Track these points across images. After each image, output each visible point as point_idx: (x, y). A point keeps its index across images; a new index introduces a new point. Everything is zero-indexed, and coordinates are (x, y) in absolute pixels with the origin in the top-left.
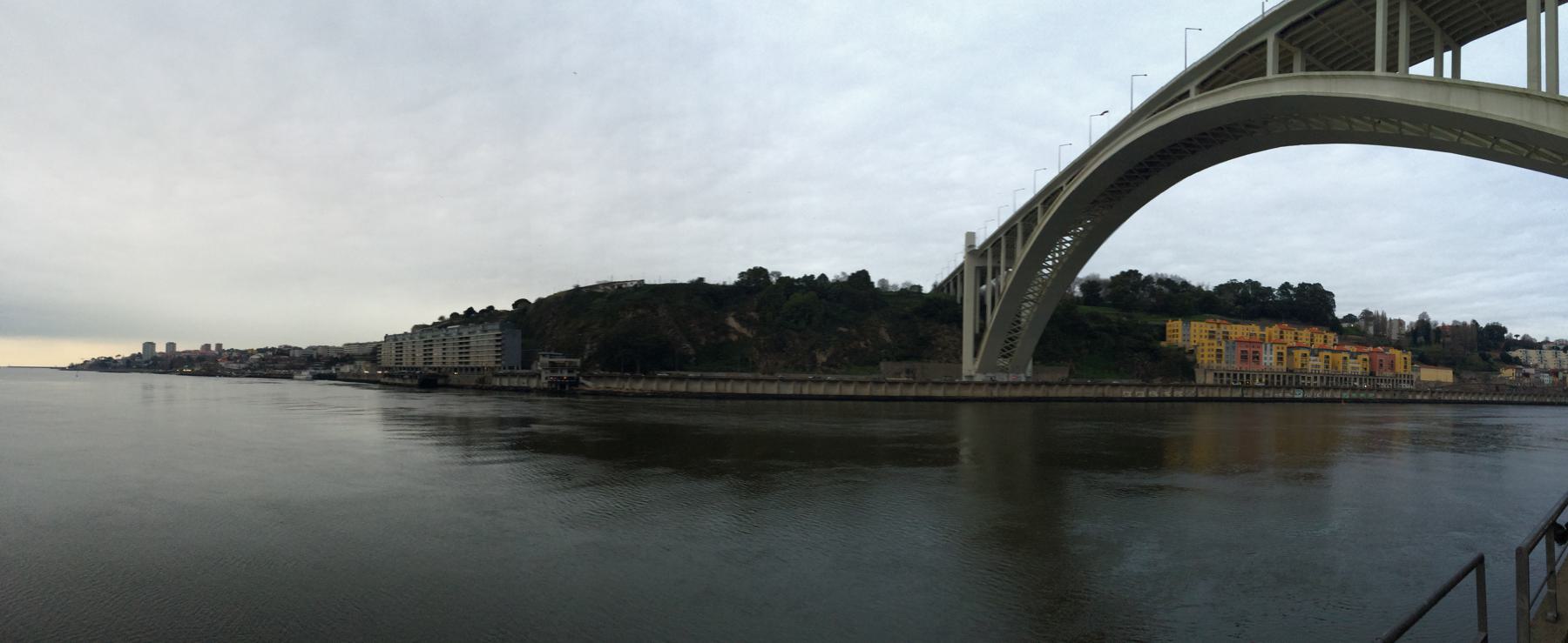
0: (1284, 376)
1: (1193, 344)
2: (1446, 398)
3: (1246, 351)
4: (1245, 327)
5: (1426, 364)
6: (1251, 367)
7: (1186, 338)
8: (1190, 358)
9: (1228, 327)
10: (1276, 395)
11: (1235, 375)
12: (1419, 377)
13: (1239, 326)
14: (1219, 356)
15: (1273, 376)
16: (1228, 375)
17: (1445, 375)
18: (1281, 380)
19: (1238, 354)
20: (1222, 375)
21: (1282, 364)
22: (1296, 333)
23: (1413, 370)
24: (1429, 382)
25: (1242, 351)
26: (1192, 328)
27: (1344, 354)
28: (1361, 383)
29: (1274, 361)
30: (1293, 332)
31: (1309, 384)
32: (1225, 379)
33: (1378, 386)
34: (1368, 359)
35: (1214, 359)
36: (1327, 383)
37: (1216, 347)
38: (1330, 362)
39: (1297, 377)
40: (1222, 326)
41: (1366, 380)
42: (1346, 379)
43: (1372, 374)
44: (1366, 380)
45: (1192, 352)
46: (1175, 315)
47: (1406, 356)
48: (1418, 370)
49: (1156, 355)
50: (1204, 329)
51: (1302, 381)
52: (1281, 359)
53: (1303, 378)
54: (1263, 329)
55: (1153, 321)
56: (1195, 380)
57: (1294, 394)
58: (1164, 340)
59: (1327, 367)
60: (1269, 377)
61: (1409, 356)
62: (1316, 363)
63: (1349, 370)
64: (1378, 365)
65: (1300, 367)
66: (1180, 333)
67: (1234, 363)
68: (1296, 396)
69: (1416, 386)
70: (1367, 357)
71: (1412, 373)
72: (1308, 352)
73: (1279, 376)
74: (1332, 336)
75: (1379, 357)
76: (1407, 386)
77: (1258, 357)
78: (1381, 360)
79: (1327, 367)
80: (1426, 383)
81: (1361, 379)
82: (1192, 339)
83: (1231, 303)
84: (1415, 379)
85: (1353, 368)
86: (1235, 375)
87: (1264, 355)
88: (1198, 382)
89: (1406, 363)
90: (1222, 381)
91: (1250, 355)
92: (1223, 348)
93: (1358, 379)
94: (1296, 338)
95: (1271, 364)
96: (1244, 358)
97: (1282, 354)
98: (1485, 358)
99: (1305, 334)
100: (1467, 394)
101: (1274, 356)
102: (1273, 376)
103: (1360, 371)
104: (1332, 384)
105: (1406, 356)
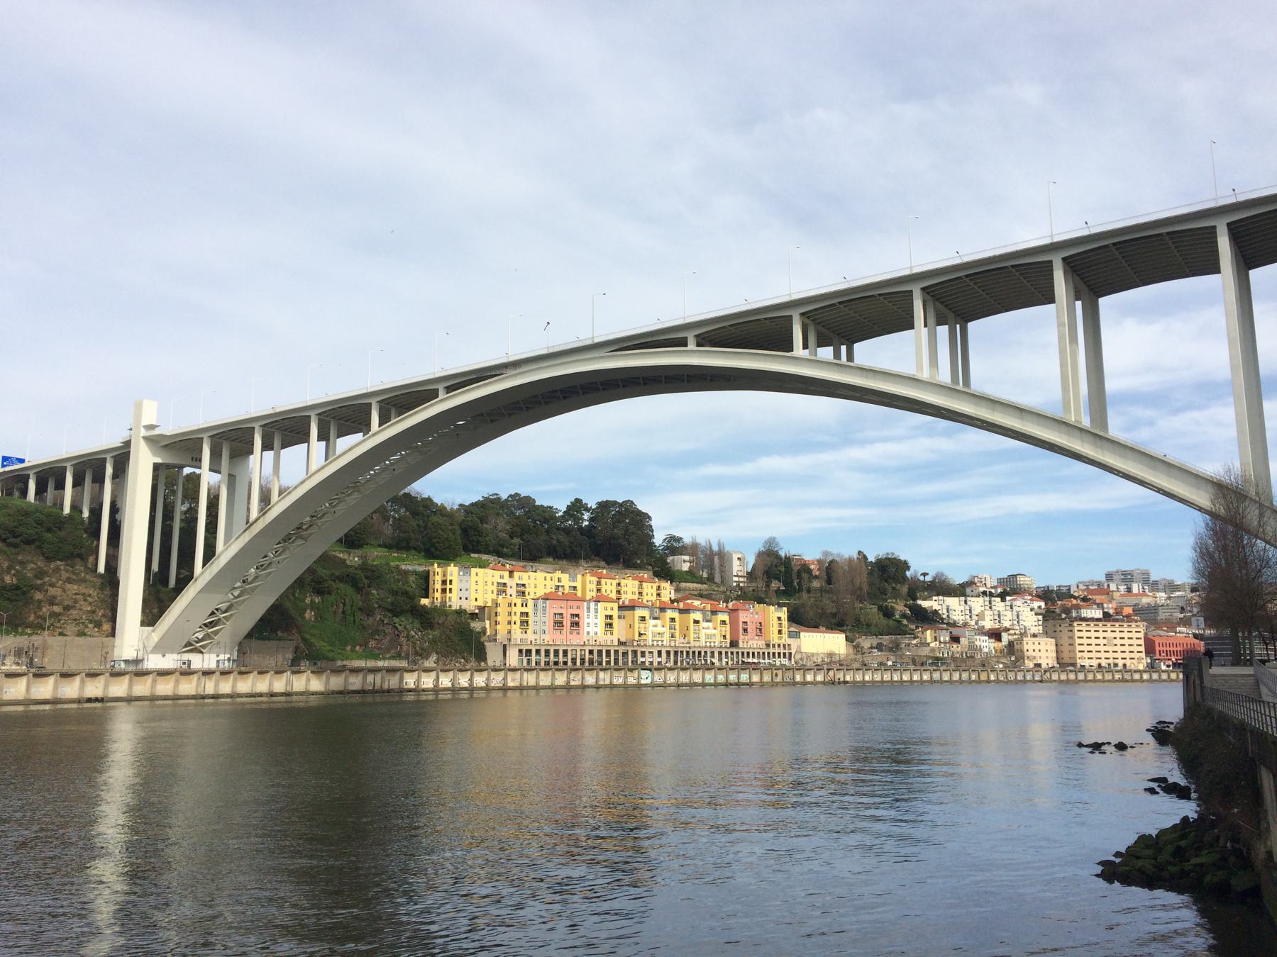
0: (616, 652)
1: (474, 603)
3: (562, 614)
4: (549, 576)
5: (808, 626)
6: (564, 639)
7: (464, 594)
8: (476, 625)
9: (525, 575)
10: (615, 682)
11: (547, 652)
12: (799, 647)
13: (540, 575)
14: (525, 623)
15: (600, 652)
16: (538, 652)
18: (612, 658)
19: (549, 620)
20: (529, 652)
21: (612, 634)
22: (619, 584)
23: (790, 636)
24: (813, 655)
26: (473, 577)
27: (698, 616)
28: (720, 659)
29: (601, 628)
30: (615, 582)
31: (651, 663)
32: (534, 657)
33: (743, 661)
34: (728, 622)
35: (516, 629)
36: (676, 662)
37: (519, 609)
38: (677, 627)
39: (635, 652)
40: (516, 574)
41: (726, 653)
42: (700, 653)
43: (734, 644)
44: (726, 653)
45: (474, 616)
46: (446, 555)
47: (779, 614)
49: (426, 618)
50: (490, 580)
51: (641, 659)
52: (611, 625)
53: (643, 654)
54: (573, 579)
55: (413, 565)
56: (485, 660)
57: (639, 678)
58: (427, 596)
59: (673, 636)
60: (595, 653)
61: (783, 613)
62: (656, 632)
63: (703, 639)
64: (741, 631)
65: (637, 637)
66: (455, 587)
67: (544, 632)
68: (643, 682)
70: (725, 617)
72: (646, 613)
73: (608, 652)
74: (668, 591)
76: (785, 661)
77: (577, 624)
78: (745, 623)
79: (673, 636)
80: (809, 656)
81: (720, 653)
82: (473, 596)
83: (504, 535)
84: (793, 651)
85: (708, 636)
86: (547, 652)
87: (586, 621)
88: (490, 663)
90: (529, 662)
91: (567, 622)
92: (530, 609)
93: (716, 655)
94: (618, 592)
95: (596, 633)
96: (558, 624)
97: (611, 617)
98: (888, 613)
99: (630, 585)
101: (601, 621)
102: (600, 652)
103: (717, 641)
104: (682, 662)
105: (779, 614)
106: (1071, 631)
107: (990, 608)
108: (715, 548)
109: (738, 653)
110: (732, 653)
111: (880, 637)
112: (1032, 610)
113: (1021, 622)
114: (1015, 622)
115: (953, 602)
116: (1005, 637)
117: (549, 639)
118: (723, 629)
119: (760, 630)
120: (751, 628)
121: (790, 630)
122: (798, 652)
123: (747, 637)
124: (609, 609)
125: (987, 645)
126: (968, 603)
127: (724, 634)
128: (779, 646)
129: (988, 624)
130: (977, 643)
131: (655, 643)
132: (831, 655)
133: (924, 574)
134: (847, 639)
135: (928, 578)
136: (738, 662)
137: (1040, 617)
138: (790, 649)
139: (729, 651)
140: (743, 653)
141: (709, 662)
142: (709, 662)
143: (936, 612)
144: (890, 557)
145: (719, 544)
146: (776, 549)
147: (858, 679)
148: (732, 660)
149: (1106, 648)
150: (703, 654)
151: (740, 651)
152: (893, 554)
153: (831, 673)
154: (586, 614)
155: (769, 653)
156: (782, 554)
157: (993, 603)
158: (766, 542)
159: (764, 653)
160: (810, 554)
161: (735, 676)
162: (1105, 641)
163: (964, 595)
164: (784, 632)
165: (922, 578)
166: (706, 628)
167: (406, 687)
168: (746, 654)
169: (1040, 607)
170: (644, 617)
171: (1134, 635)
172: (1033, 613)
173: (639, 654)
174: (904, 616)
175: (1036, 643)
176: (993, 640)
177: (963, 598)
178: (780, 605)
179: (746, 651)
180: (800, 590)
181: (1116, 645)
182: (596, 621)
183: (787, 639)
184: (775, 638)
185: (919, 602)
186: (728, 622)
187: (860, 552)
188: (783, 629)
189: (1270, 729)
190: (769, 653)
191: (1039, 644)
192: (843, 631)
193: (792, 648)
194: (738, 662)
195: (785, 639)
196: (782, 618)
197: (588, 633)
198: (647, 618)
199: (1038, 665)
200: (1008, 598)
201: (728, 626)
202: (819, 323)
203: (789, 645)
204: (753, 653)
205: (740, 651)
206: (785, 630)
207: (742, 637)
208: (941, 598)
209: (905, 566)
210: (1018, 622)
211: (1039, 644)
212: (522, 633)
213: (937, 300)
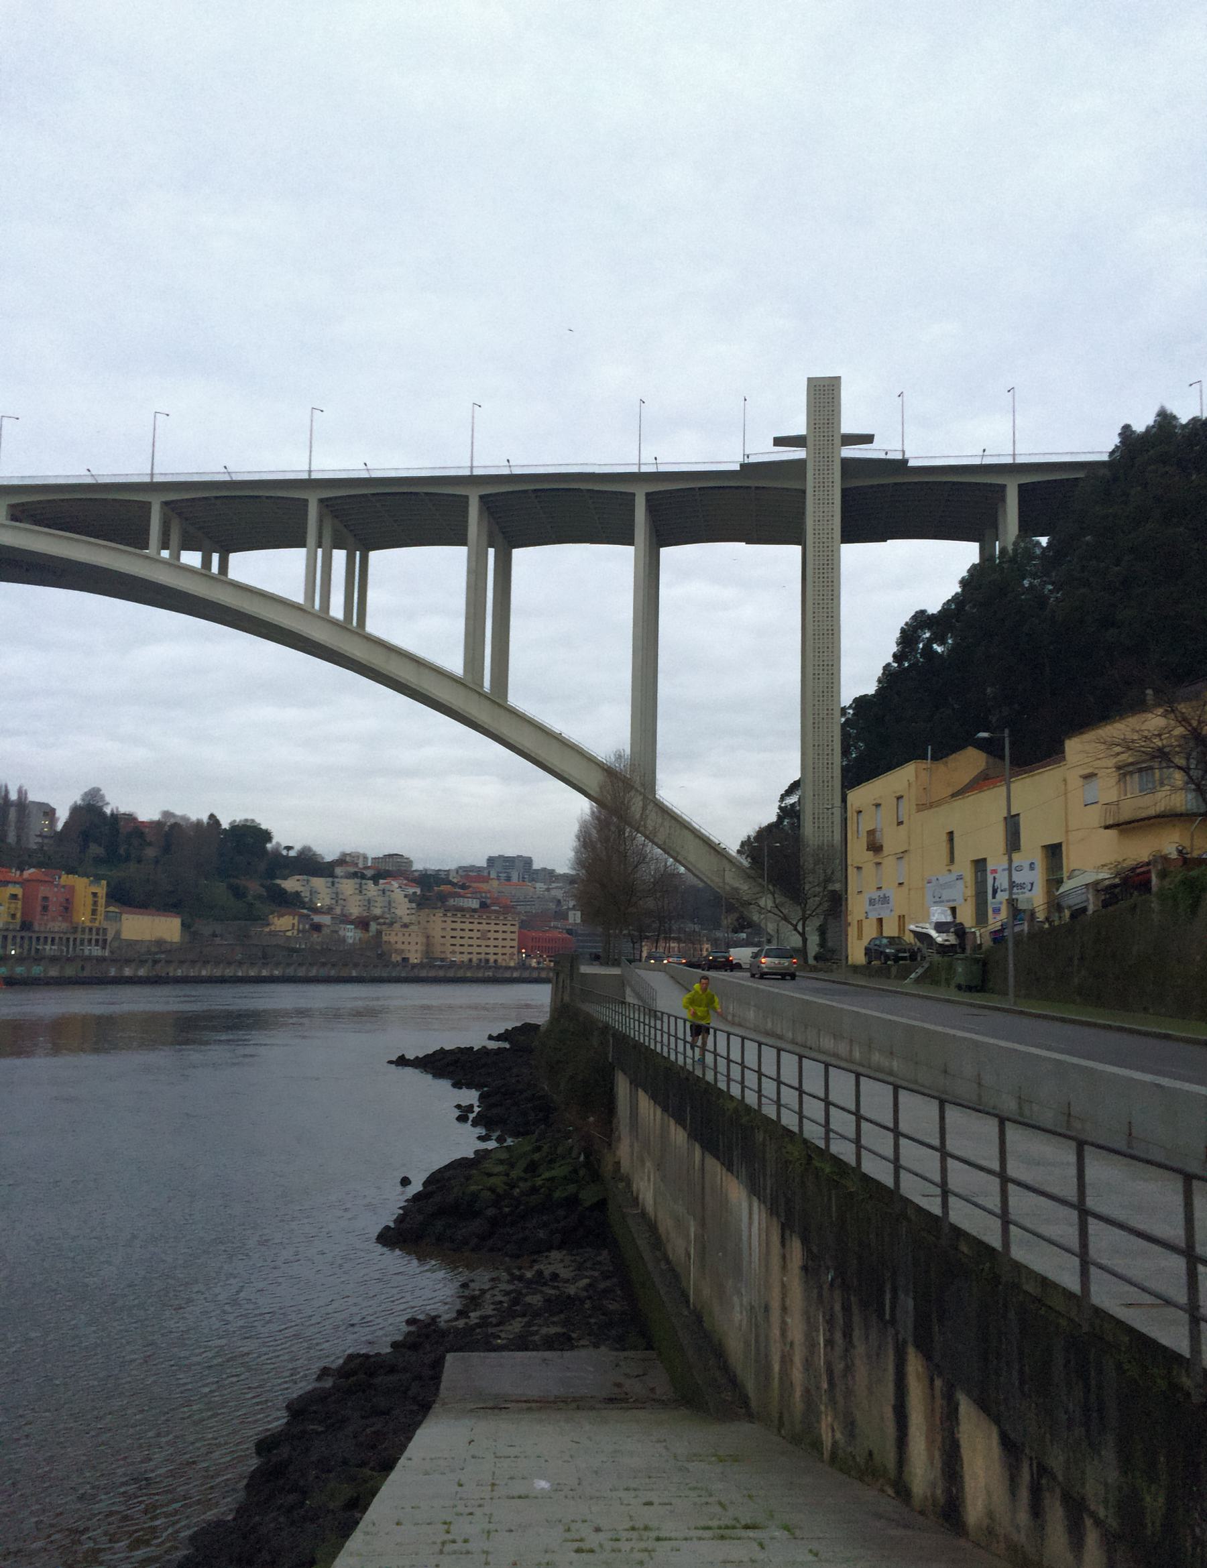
2: (179, 973)
5: (130, 905)
17: (168, 928)
23: (107, 918)
34: (20, 896)
41: (14, 937)
43: (26, 926)
48: (117, 918)
61: (102, 889)
64: (39, 909)
69: (112, 952)
70: (18, 890)
71: (105, 925)
75: (43, 891)
76: (97, 951)
78: (45, 898)
80: (132, 944)
84: (109, 939)
89: (95, 903)
98: (238, 893)
100: (217, 963)
106: (445, 921)
107: (361, 892)
108: (13, 796)
109: (31, 938)
110: (22, 938)
111: (226, 922)
112: (406, 896)
113: (393, 910)
114: (386, 909)
115: (319, 883)
116: (373, 927)
118: (13, 906)
119: (67, 909)
120: (52, 908)
121: (108, 909)
123: (46, 918)
125: (351, 934)
126: (336, 885)
127: (13, 912)
128: (91, 929)
129: (355, 911)
130: (341, 933)
132: (160, 943)
133: (289, 848)
134: (183, 924)
135: (292, 853)
136: (30, 950)
137: (414, 905)
138: (106, 935)
139: (19, 935)
143: (297, 894)
144: (248, 824)
145: (20, 791)
146: (100, 804)
147: (192, 974)
148: (21, 946)
149: (479, 942)
151: (34, 936)
152: (253, 821)
153: (158, 967)
155: (75, 939)
156: (108, 810)
157: (364, 887)
158: (86, 794)
159: (68, 939)
160: (147, 813)
161: (23, 968)
162: (479, 934)
163: (332, 875)
164: (99, 913)
165: (284, 852)
168: (42, 940)
169: (415, 893)
171: (508, 928)
172: (407, 900)
174: (259, 897)
175: (407, 934)
176: (359, 931)
177: (330, 879)
178: (98, 878)
179: (43, 935)
180: (127, 859)
181: (489, 939)
184: (83, 918)
185: (278, 881)
186: (20, 896)
187: (212, 816)
188: (99, 908)
189: (665, 1049)
190: (75, 939)
191: (410, 935)
192: (178, 914)
194: (30, 950)
196: (99, 895)
199: (405, 960)
200: (381, 881)
201: (20, 903)
203: (105, 930)
204: (53, 940)
205: (34, 936)
206: (101, 909)
207: (38, 917)
208: (305, 877)
209: (266, 836)
210: (389, 910)
211: (410, 935)
213: (337, 517)
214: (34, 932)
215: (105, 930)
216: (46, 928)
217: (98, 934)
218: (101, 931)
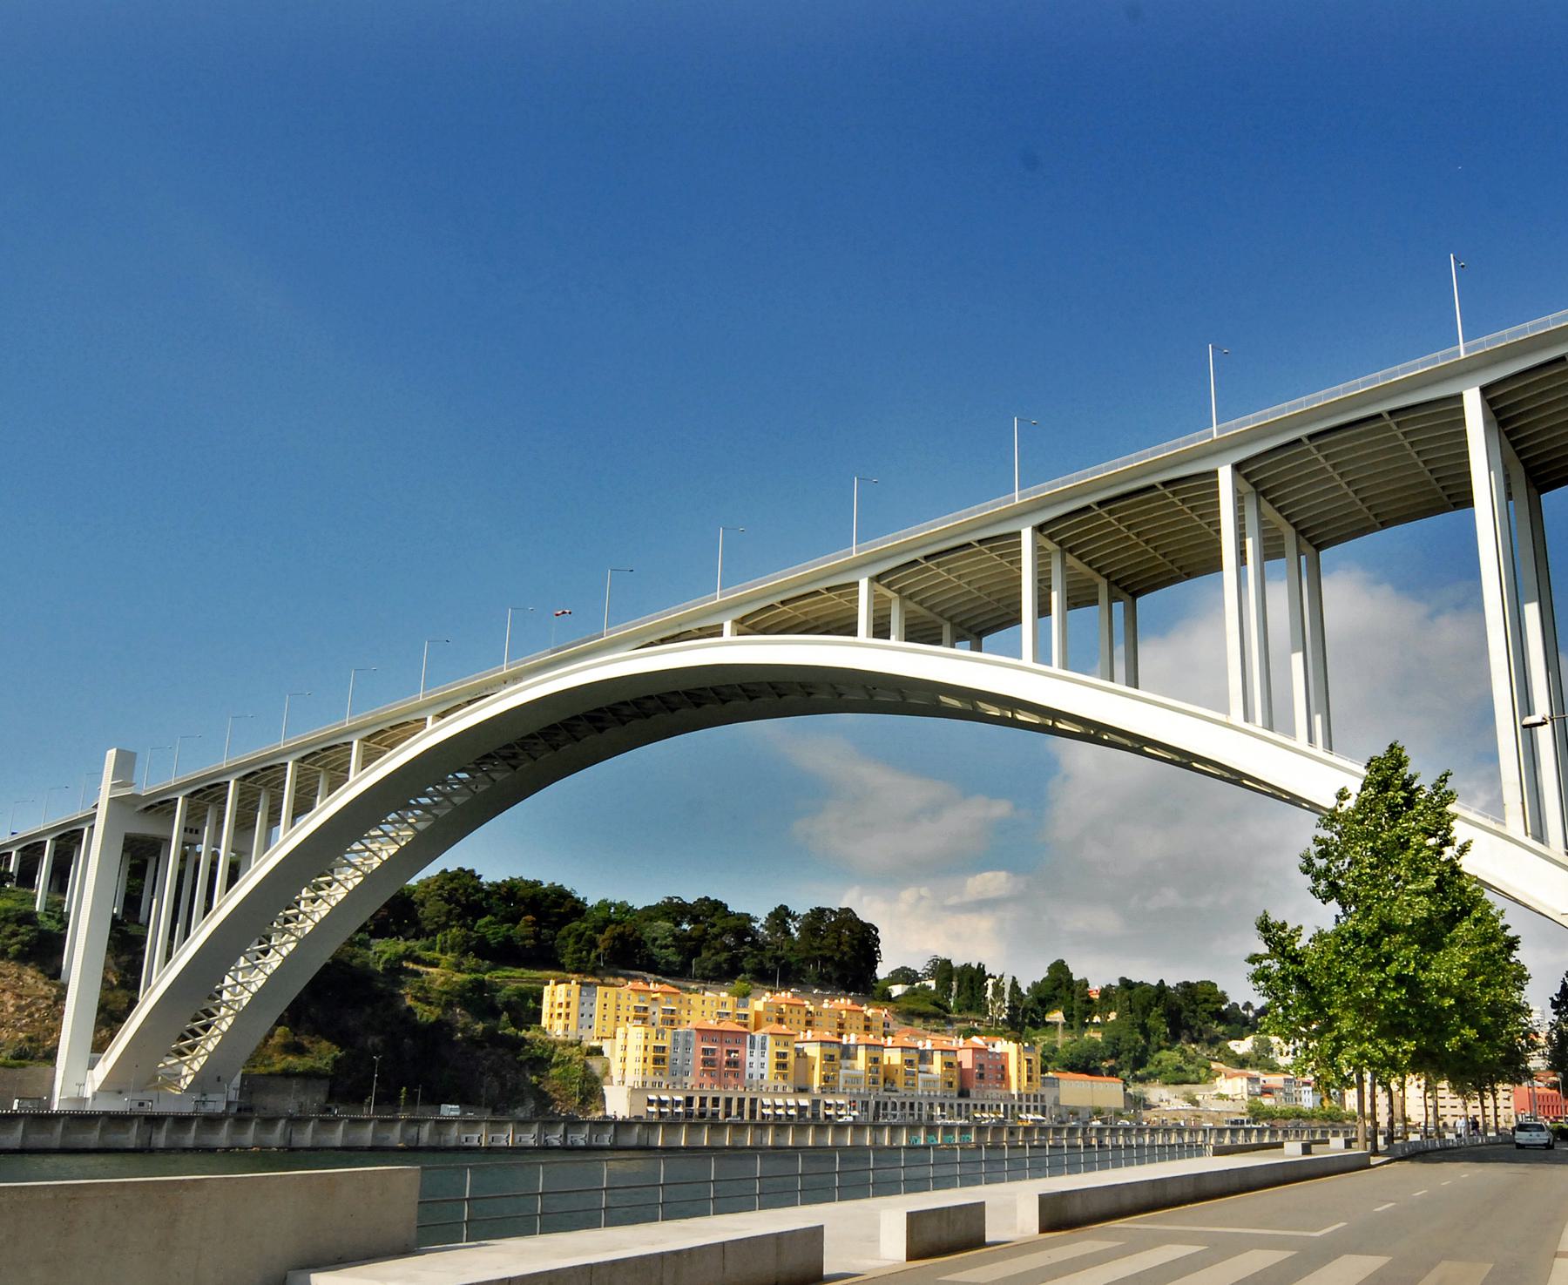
12: (1057, 1099)
23: (1044, 1085)
25: (705, 1051)
48: (1054, 1083)
52: (784, 1066)
71: (1043, 1091)
87: (748, 1059)
89: (1030, 1070)
109: (967, 1105)
110: (959, 1105)
117: (693, 1083)
122: (1057, 1104)
124: (782, 1043)
131: (848, 1090)
138: (1042, 1101)
140: (975, 1106)
141: (924, 1117)
142: (924, 1117)
150: (916, 1105)
151: (971, 1103)
154: (748, 1050)
155: (1013, 1107)
166: (924, 1072)
167: (466, 1144)
168: (979, 1107)
170: (833, 1056)
173: (822, 1105)
182: (762, 1060)
183: (1039, 1087)
193: (1046, 1098)
195: (1037, 1088)
197: (751, 1076)
198: (837, 1057)
202: (911, 597)
205: (971, 1103)
212: (655, 1074)
214: (972, 1099)
215: (1042, 1096)
216: (983, 1096)
217: (1036, 1101)
218: (1039, 1097)
